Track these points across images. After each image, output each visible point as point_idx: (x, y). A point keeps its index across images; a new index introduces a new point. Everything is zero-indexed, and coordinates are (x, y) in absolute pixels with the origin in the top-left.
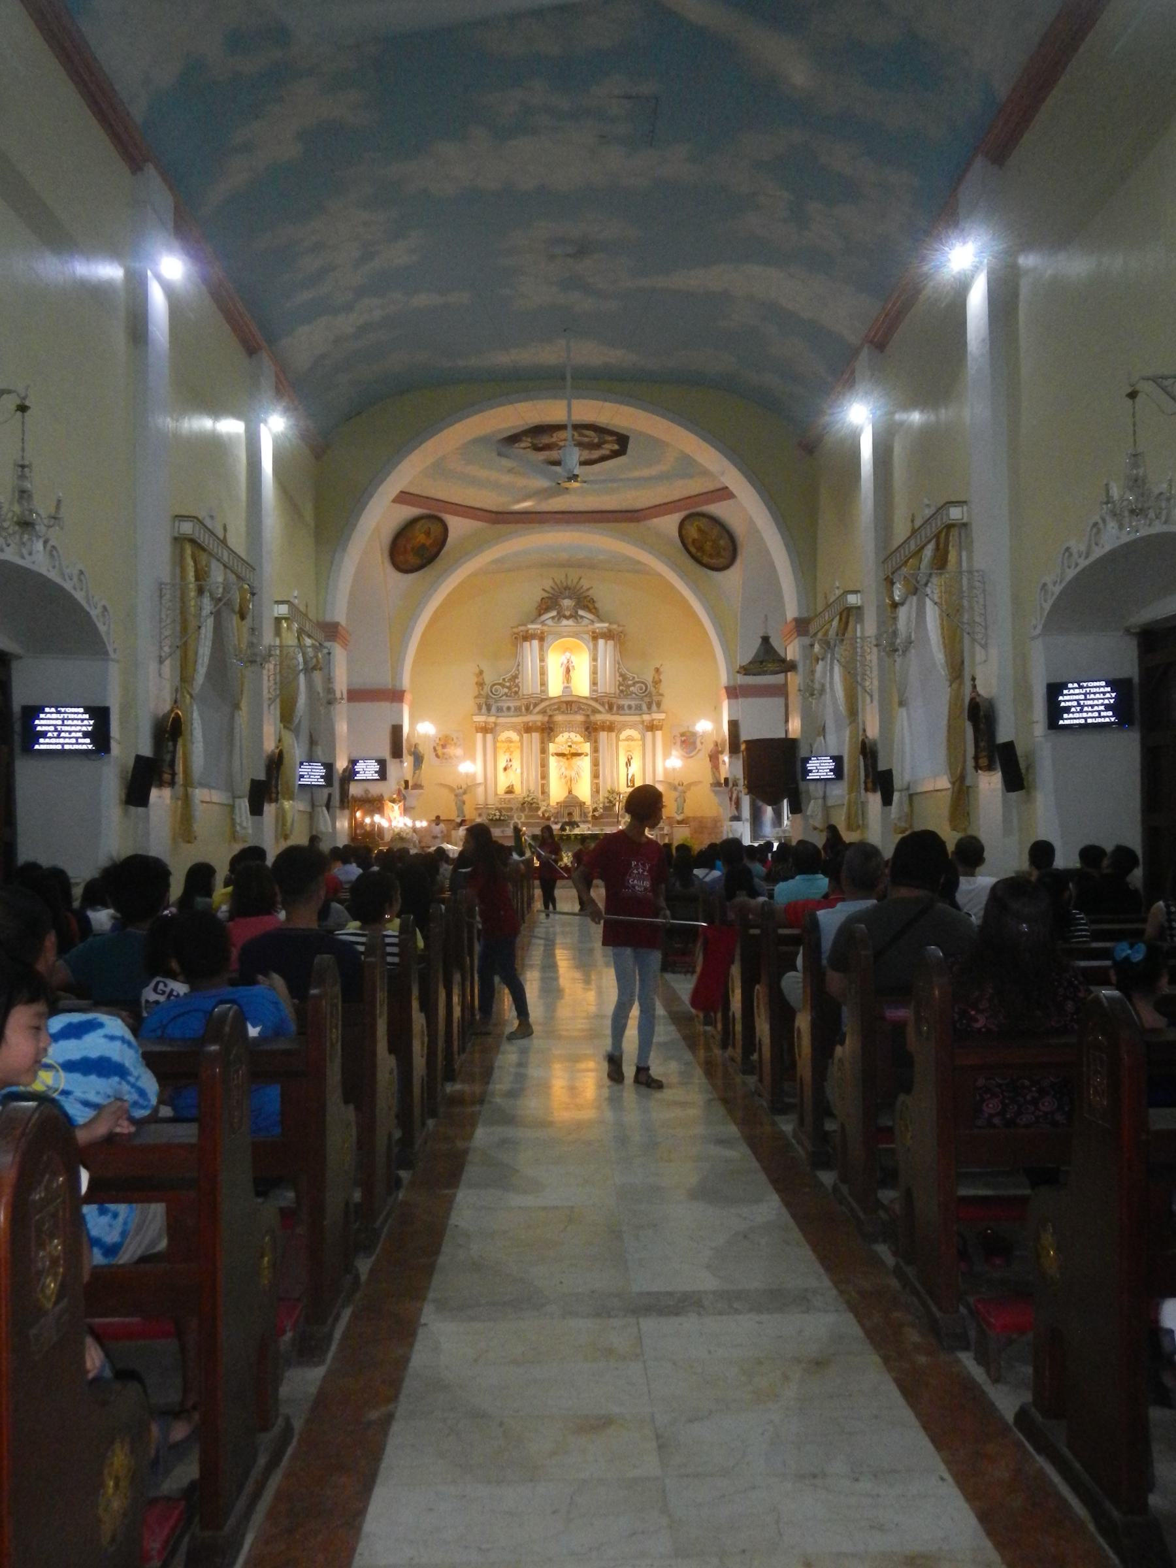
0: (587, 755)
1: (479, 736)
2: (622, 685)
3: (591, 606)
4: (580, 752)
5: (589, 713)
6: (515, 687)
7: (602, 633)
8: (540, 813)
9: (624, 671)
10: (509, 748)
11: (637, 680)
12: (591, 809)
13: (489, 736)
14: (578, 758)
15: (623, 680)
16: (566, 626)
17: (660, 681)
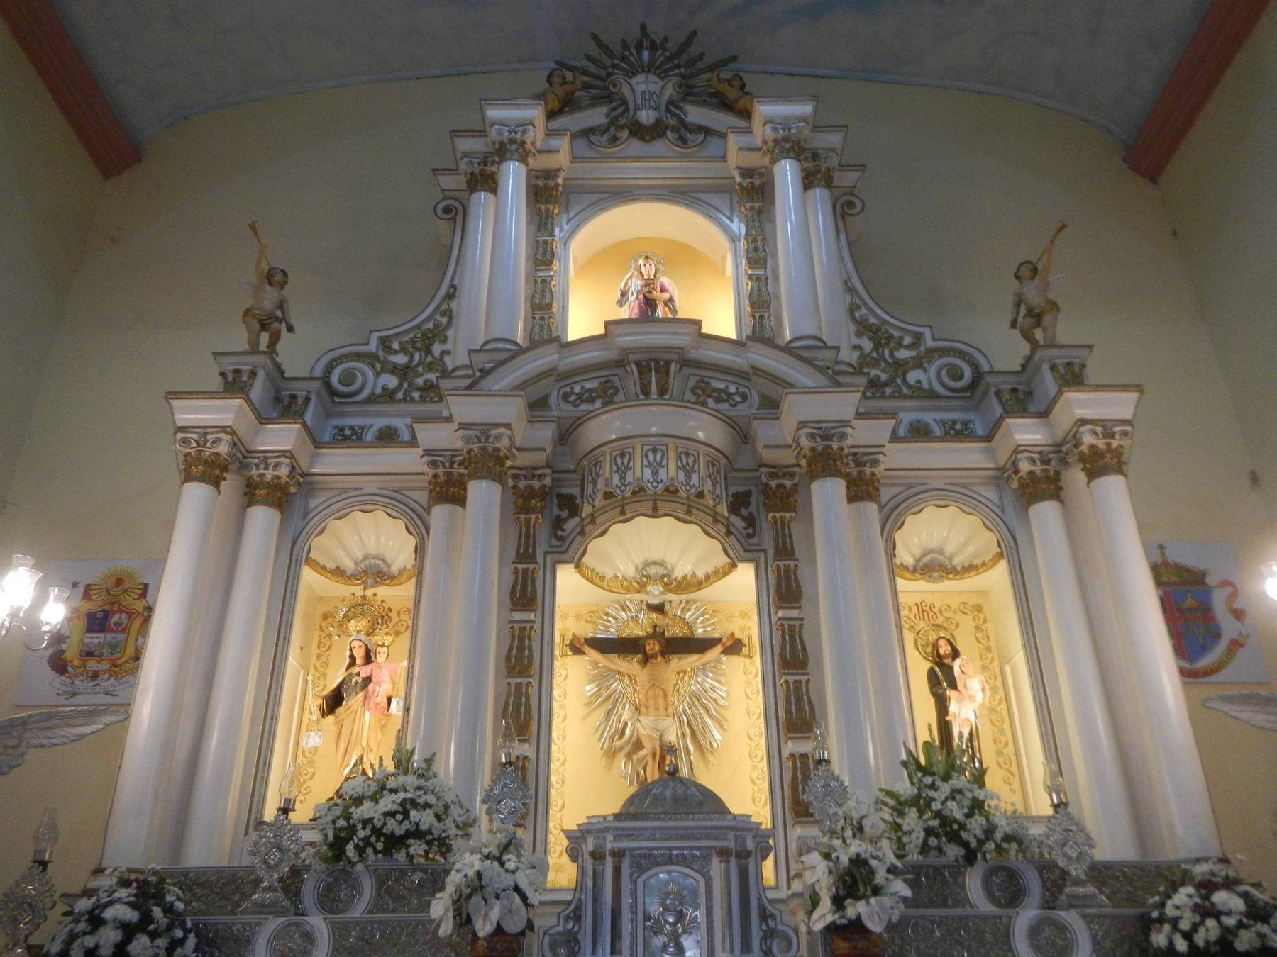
0: (734, 647)
1: (195, 494)
2: (875, 363)
3: (732, 93)
4: (700, 632)
5: (743, 410)
6: (430, 368)
7: (786, 139)
8: (440, 907)
9: (876, 314)
10: (359, 607)
11: (930, 343)
12: (819, 874)
13: (262, 519)
14: (693, 660)
15: (877, 345)
16: (638, 159)
17: (1054, 307)
